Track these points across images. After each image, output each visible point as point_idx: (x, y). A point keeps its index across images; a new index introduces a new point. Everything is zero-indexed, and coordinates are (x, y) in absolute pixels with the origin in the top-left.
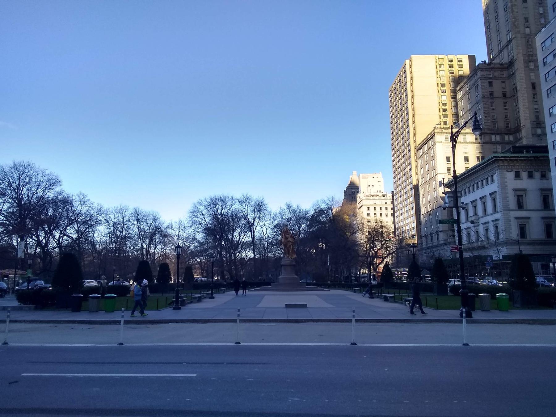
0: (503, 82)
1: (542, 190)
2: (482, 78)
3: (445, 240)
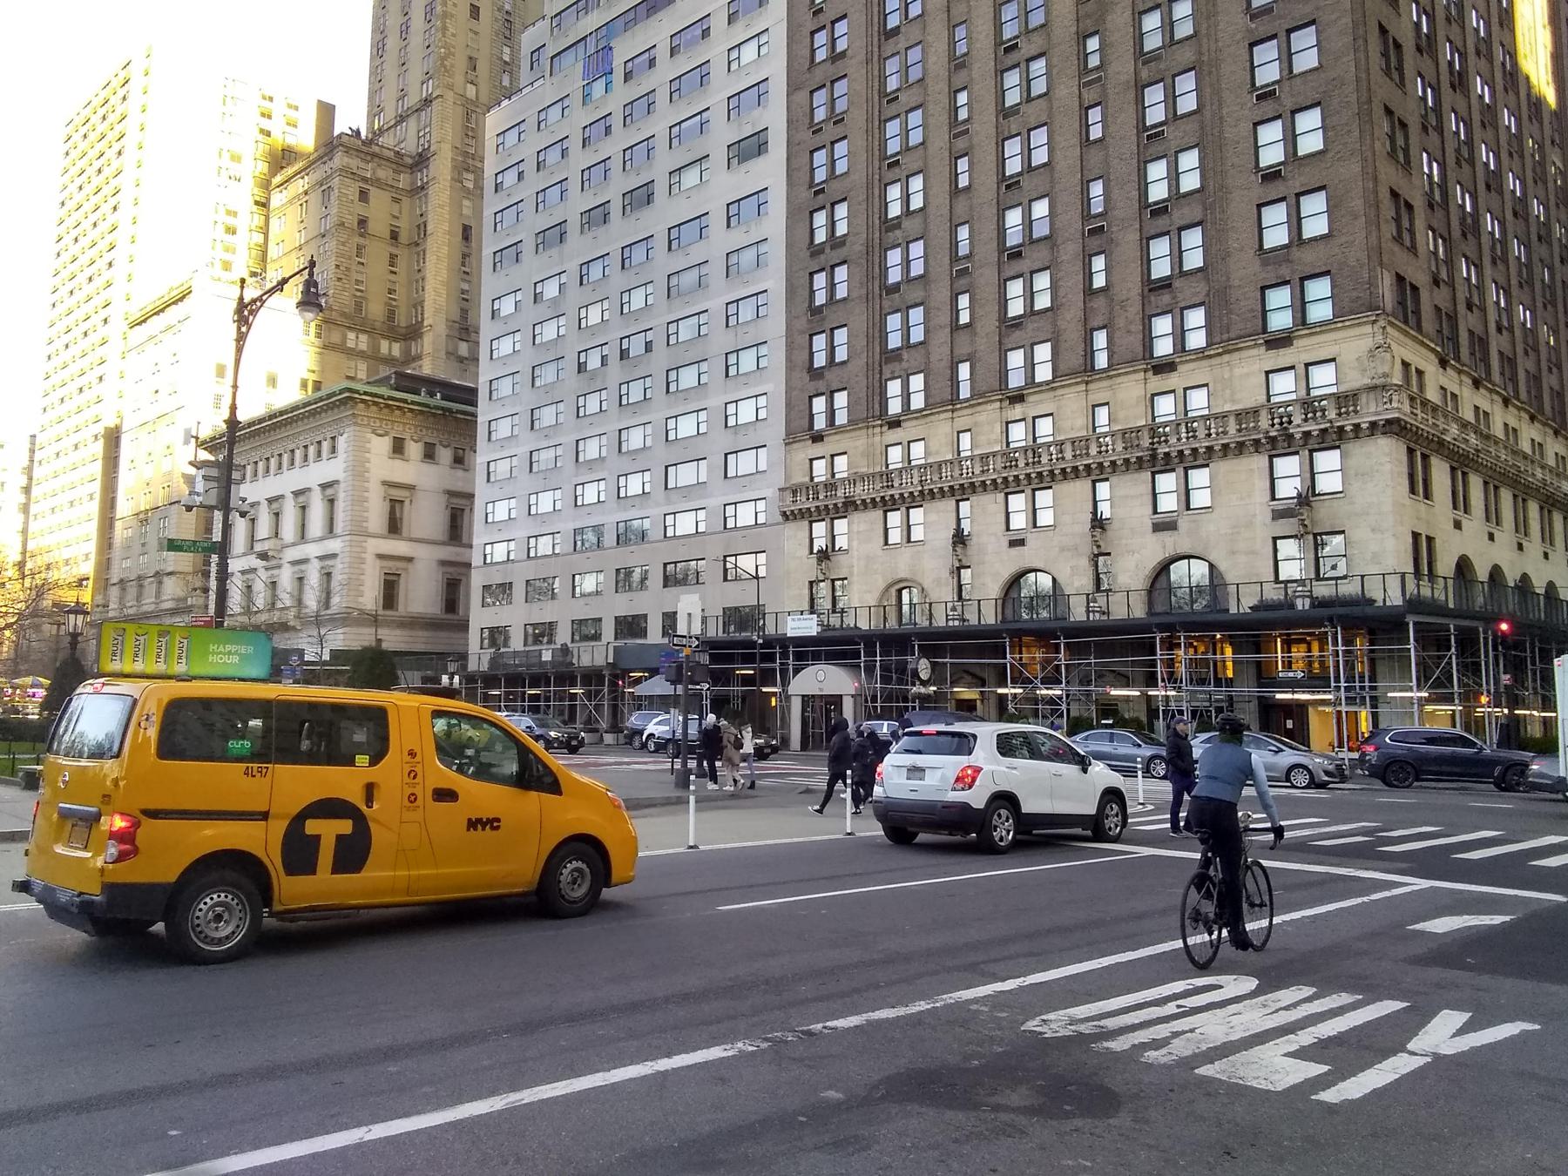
0: (396, 200)
1: (451, 494)
2: (346, 172)
3: (178, 600)
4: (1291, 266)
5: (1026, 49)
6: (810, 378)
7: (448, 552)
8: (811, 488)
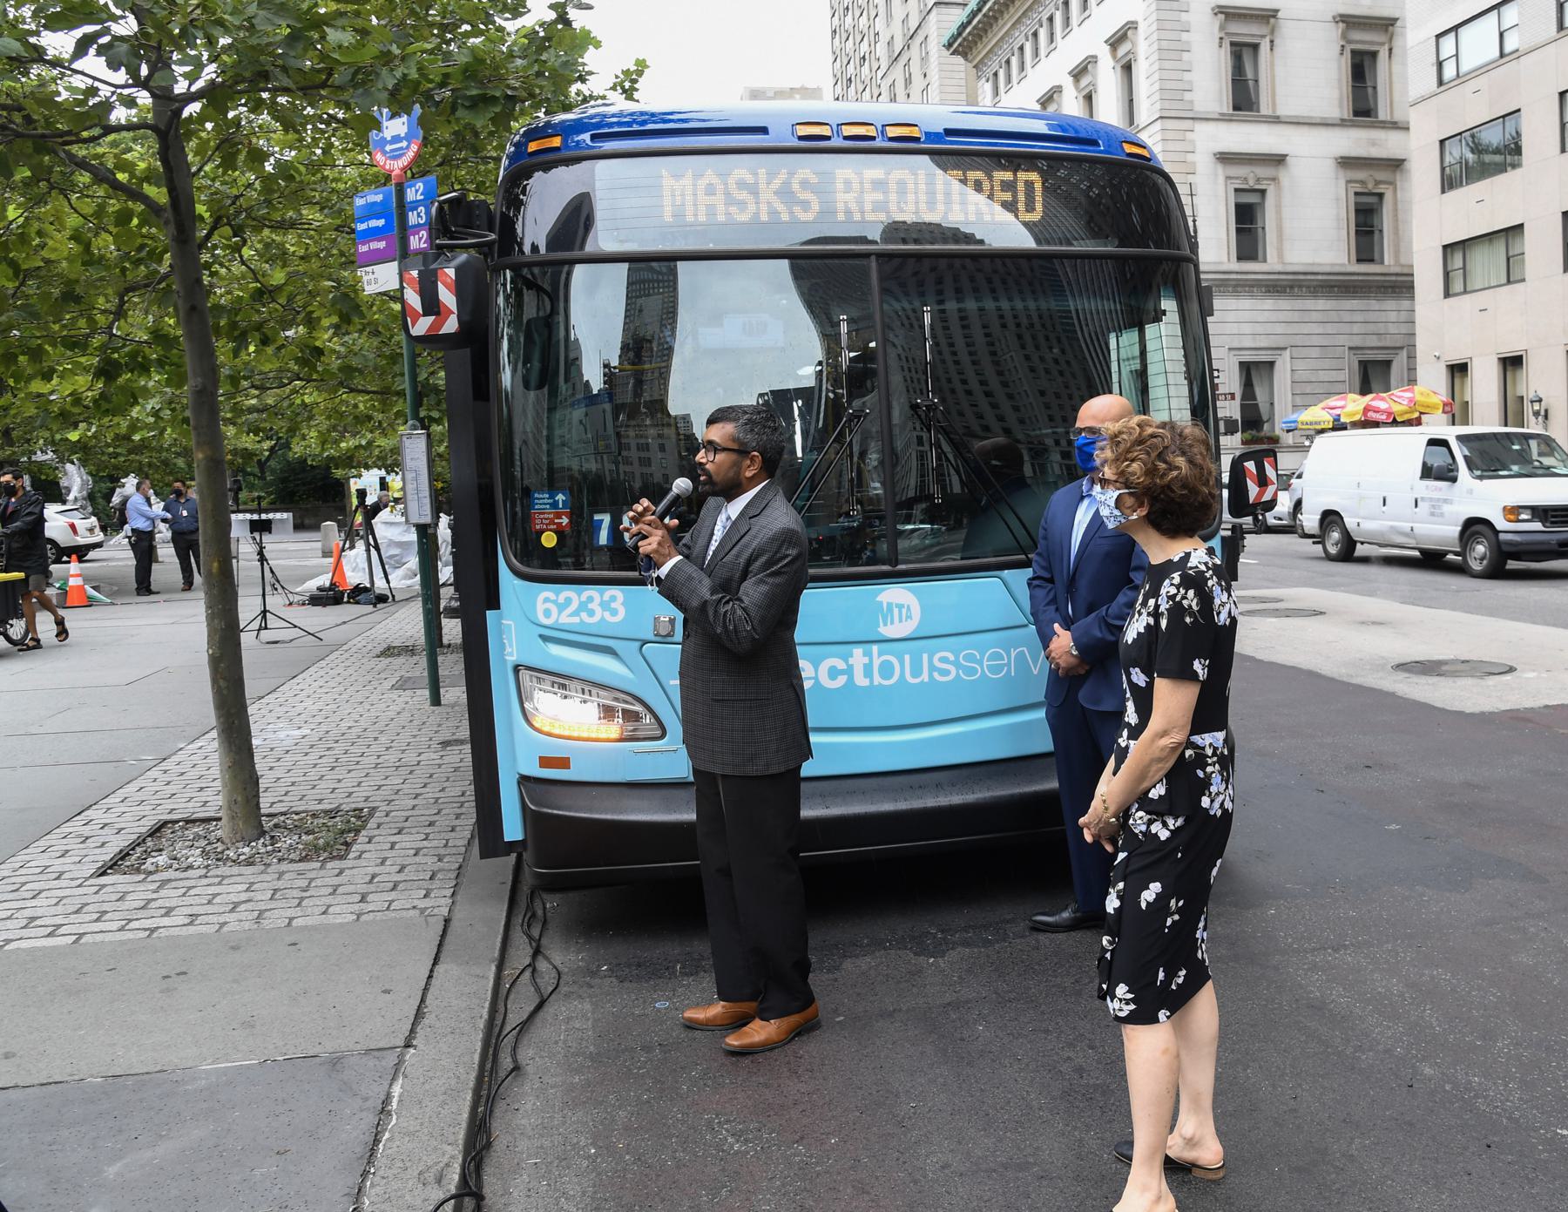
1: (1349, 22)
7: (1356, 142)
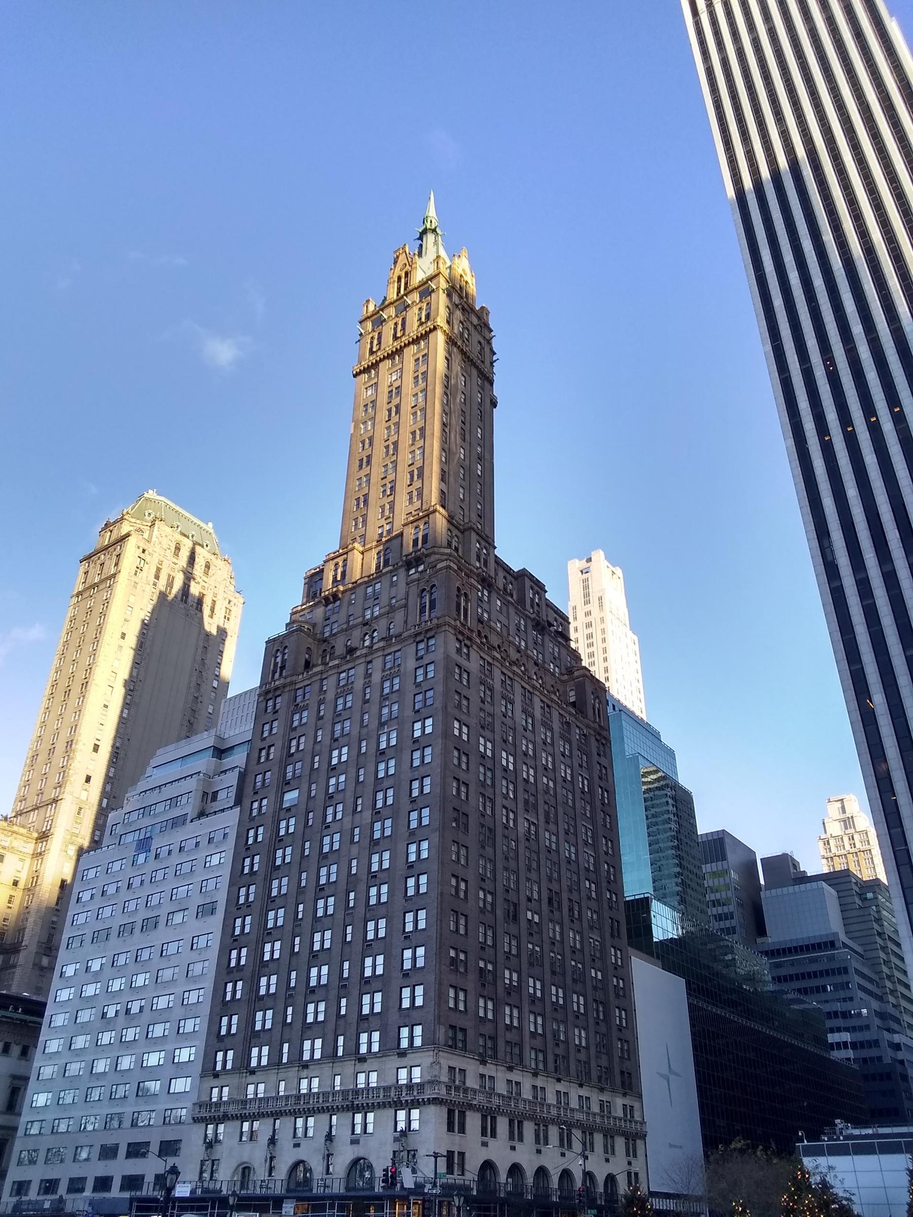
0: (22, 860)
1: (14, 1077)
4: (409, 1017)
5: (328, 891)
6: (217, 1040)
8: (209, 1105)
